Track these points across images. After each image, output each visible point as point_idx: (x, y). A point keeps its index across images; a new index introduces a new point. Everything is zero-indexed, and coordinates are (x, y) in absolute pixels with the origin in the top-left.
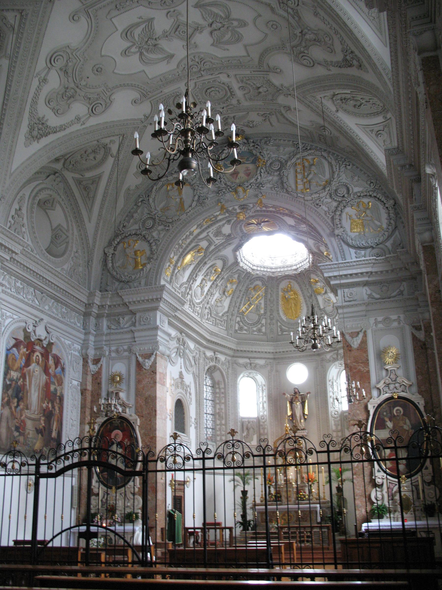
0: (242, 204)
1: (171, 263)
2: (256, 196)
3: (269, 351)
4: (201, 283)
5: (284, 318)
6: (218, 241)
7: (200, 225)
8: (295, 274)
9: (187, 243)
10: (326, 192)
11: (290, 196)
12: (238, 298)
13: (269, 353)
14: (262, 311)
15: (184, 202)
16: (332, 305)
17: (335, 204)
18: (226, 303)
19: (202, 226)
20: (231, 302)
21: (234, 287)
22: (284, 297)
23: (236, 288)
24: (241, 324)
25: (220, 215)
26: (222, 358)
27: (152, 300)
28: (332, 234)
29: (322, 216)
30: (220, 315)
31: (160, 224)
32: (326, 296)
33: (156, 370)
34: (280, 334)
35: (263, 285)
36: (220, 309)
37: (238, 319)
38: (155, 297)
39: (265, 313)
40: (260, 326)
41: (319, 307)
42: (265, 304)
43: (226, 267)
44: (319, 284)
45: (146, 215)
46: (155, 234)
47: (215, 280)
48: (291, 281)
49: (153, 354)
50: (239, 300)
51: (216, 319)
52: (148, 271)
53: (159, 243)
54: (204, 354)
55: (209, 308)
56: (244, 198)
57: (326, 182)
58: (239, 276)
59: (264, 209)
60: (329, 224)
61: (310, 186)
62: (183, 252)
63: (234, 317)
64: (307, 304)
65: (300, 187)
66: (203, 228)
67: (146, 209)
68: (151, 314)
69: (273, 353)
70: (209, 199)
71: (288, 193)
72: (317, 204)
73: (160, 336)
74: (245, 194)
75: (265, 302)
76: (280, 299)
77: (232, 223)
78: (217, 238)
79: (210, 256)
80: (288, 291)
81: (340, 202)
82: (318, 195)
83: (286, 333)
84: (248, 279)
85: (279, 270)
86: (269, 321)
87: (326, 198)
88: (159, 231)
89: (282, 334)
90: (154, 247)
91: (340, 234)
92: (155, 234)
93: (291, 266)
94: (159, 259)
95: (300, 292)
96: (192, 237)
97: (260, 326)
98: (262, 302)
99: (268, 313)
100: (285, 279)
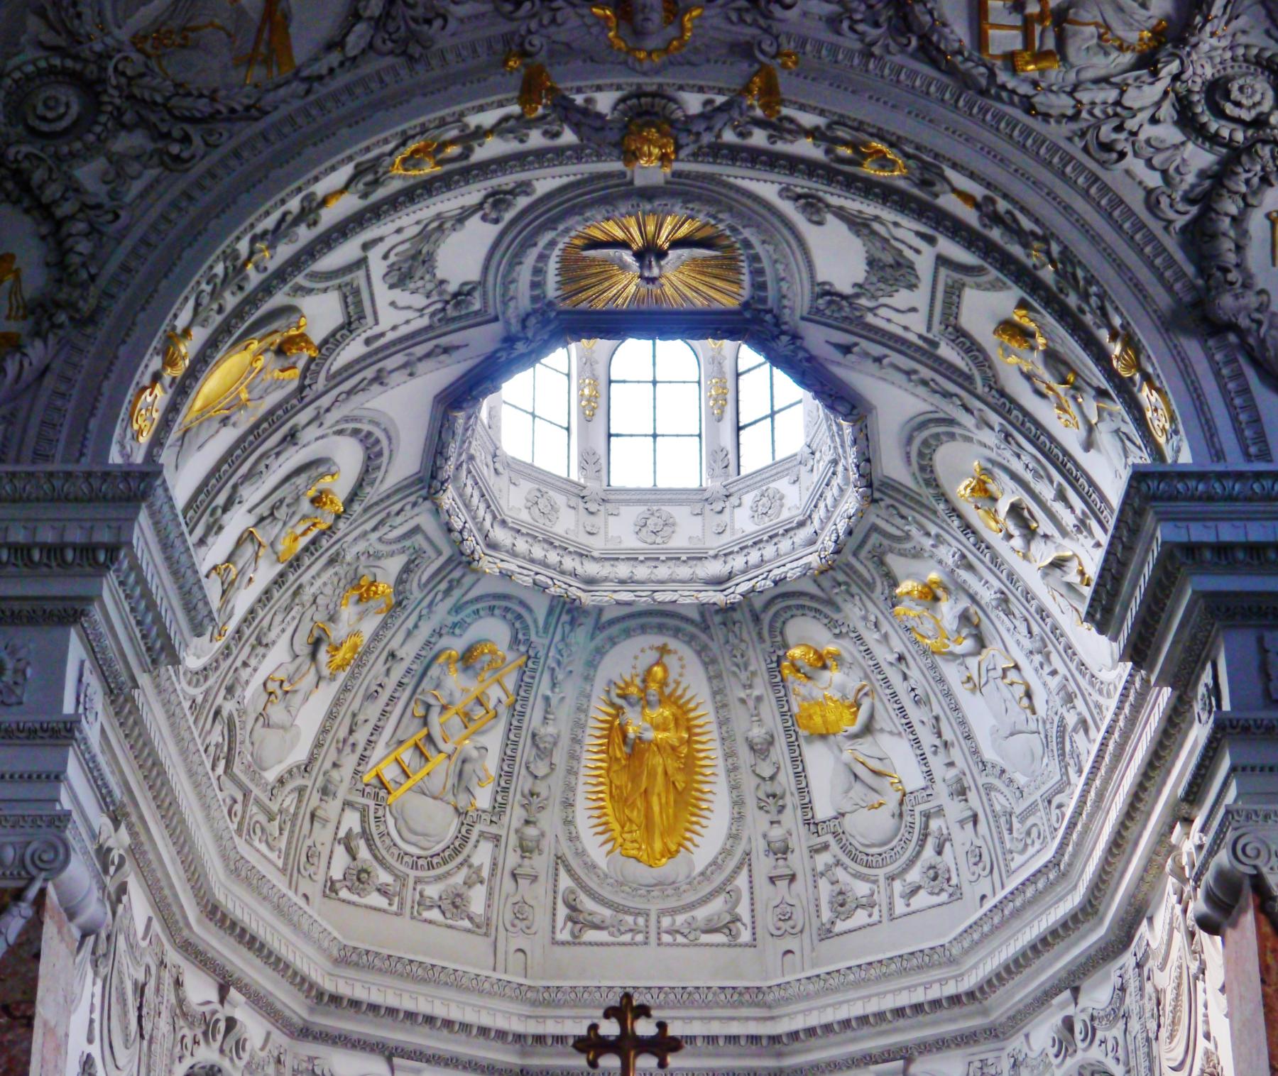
0: (650, 83)
1: (170, 362)
2: (745, 50)
3: (501, 1023)
4: (229, 559)
5: (596, 850)
6: (395, 310)
7: (374, 165)
8: (703, 608)
9: (272, 266)
10: (1161, 86)
11: (946, 79)
12: (371, 696)
13: (501, 1035)
14: (483, 798)
15: (287, 18)
16: (892, 800)
17: (1199, 158)
18: (310, 713)
19: (376, 183)
20: (331, 716)
21: (369, 626)
22: (615, 731)
23: (376, 637)
24: (364, 853)
25: (498, 129)
26: (253, 1027)
27: (54, 551)
28: (1198, 314)
29: (1130, 213)
30: (271, 776)
31: (128, 118)
32: (865, 747)
33: (31, 1002)
34: (564, 936)
35: (515, 641)
36: (270, 741)
37: (352, 821)
38: (75, 535)
39: (499, 808)
40: (459, 878)
41: (807, 806)
42: (508, 758)
43: (372, 494)
44: (835, 676)
45: (30, 53)
46: (89, 174)
47: (295, 564)
48: (673, 644)
49: (18, 895)
50: (372, 711)
51: (246, 794)
52: (28, 374)
53: (110, 230)
54: (178, 983)
55: (230, 717)
56: (666, 50)
57: (1156, 32)
58: (407, 569)
59: (759, 138)
60: (1171, 262)
61: (1061, 40)
62: (239, 313)
63: (333, 806)
64: (734, 787)
65: (1004, 39)
66: (380, 193)
67: (33, 23)
68: (30, 640)
69: (519, 1038)
70: (452, 24)
71: (934, 63)
72: (1107, 147)
73: (71, 787)
74: (671, 31)
75: (510, 744)
76: (592, 741)
77: (508, 216)
78: (397, 295)
79: (325, 401)
80: (645, 702)
81: (1234, 156)
82: (1112, 95)
83: (602, 936)
84: (447, 592)
85: (623, 570)
86: (512, 859)
87: (1154, 120)
88: (118, 162)
89: (576, 941)
90: (83, 246)
91: (1244, 322)
92: (89, 174)
93: (698, 558)
94: (107, 322)
95: (705, 714)
96: (304, 234)
97: (459, 878)
98: (494, 740)
99: (516, 815)
100: (643, 629)
